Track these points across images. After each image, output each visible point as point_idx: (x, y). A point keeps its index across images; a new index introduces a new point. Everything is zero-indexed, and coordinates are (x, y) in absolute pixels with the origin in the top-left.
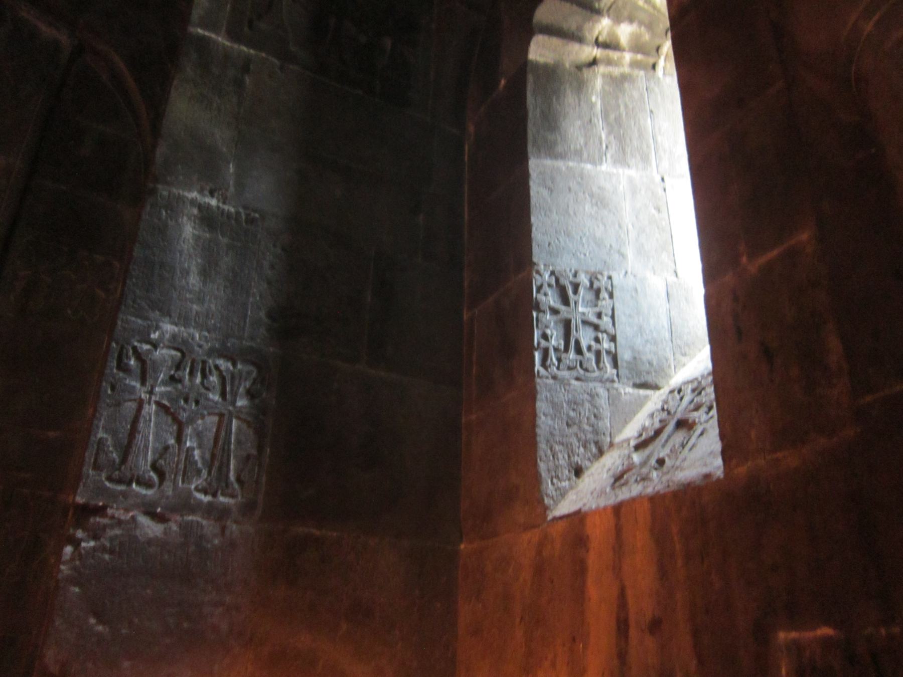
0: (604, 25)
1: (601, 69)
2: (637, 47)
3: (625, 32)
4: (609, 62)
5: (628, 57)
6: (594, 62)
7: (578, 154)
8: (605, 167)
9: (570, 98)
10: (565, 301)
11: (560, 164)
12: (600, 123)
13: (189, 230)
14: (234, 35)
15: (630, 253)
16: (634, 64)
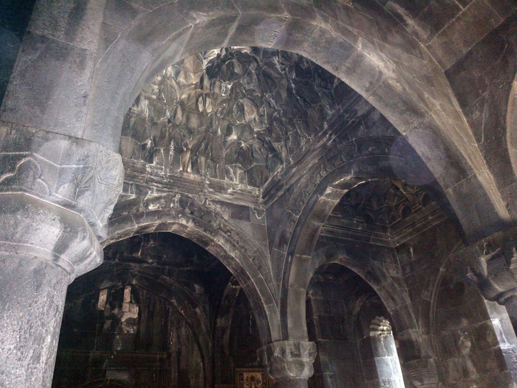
0: (381, 327)
1: (382, 336)
2: (387, 330)
3: (385, 328)
4: (383, 334)
5: (386, 332)
6: (380, 334)
7: (382, 356)
8: (386, 357)
9: (378, 343)
10: (385, 384)
11: (379, 358)
12: (384, 348)
13: (329, 380)
14: (323, 338)
15: (393, 373)
16: (387, 333)
